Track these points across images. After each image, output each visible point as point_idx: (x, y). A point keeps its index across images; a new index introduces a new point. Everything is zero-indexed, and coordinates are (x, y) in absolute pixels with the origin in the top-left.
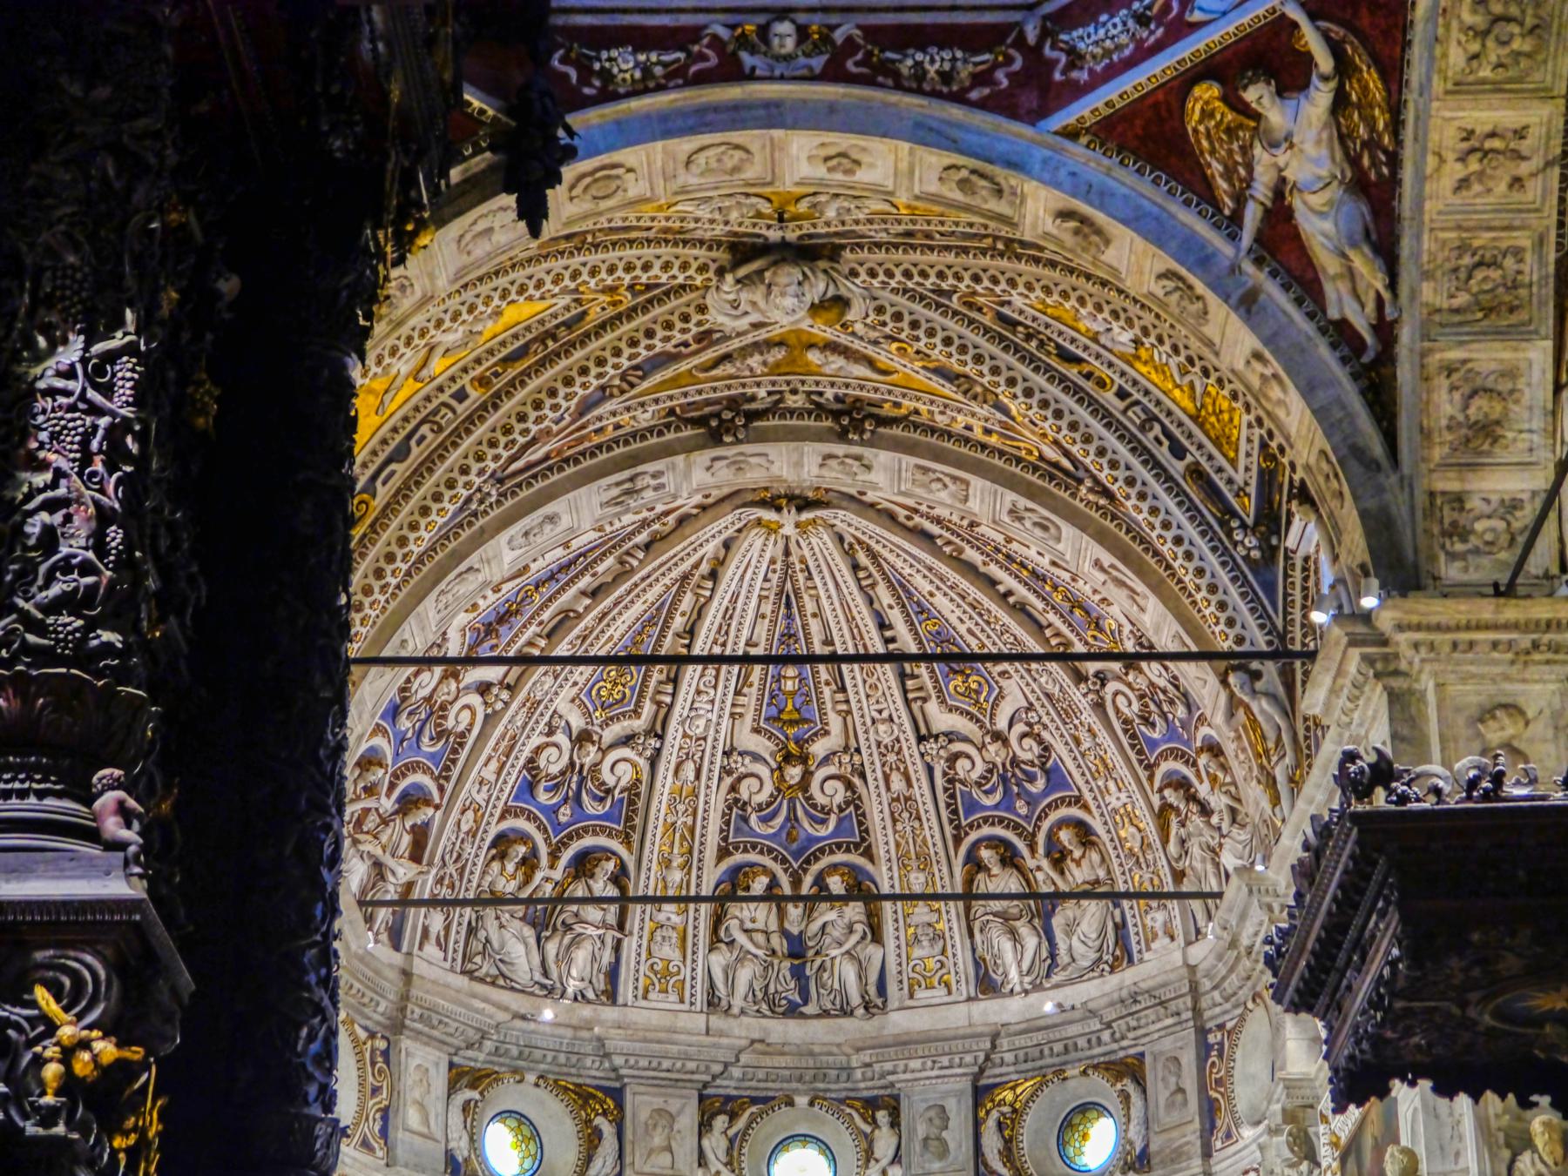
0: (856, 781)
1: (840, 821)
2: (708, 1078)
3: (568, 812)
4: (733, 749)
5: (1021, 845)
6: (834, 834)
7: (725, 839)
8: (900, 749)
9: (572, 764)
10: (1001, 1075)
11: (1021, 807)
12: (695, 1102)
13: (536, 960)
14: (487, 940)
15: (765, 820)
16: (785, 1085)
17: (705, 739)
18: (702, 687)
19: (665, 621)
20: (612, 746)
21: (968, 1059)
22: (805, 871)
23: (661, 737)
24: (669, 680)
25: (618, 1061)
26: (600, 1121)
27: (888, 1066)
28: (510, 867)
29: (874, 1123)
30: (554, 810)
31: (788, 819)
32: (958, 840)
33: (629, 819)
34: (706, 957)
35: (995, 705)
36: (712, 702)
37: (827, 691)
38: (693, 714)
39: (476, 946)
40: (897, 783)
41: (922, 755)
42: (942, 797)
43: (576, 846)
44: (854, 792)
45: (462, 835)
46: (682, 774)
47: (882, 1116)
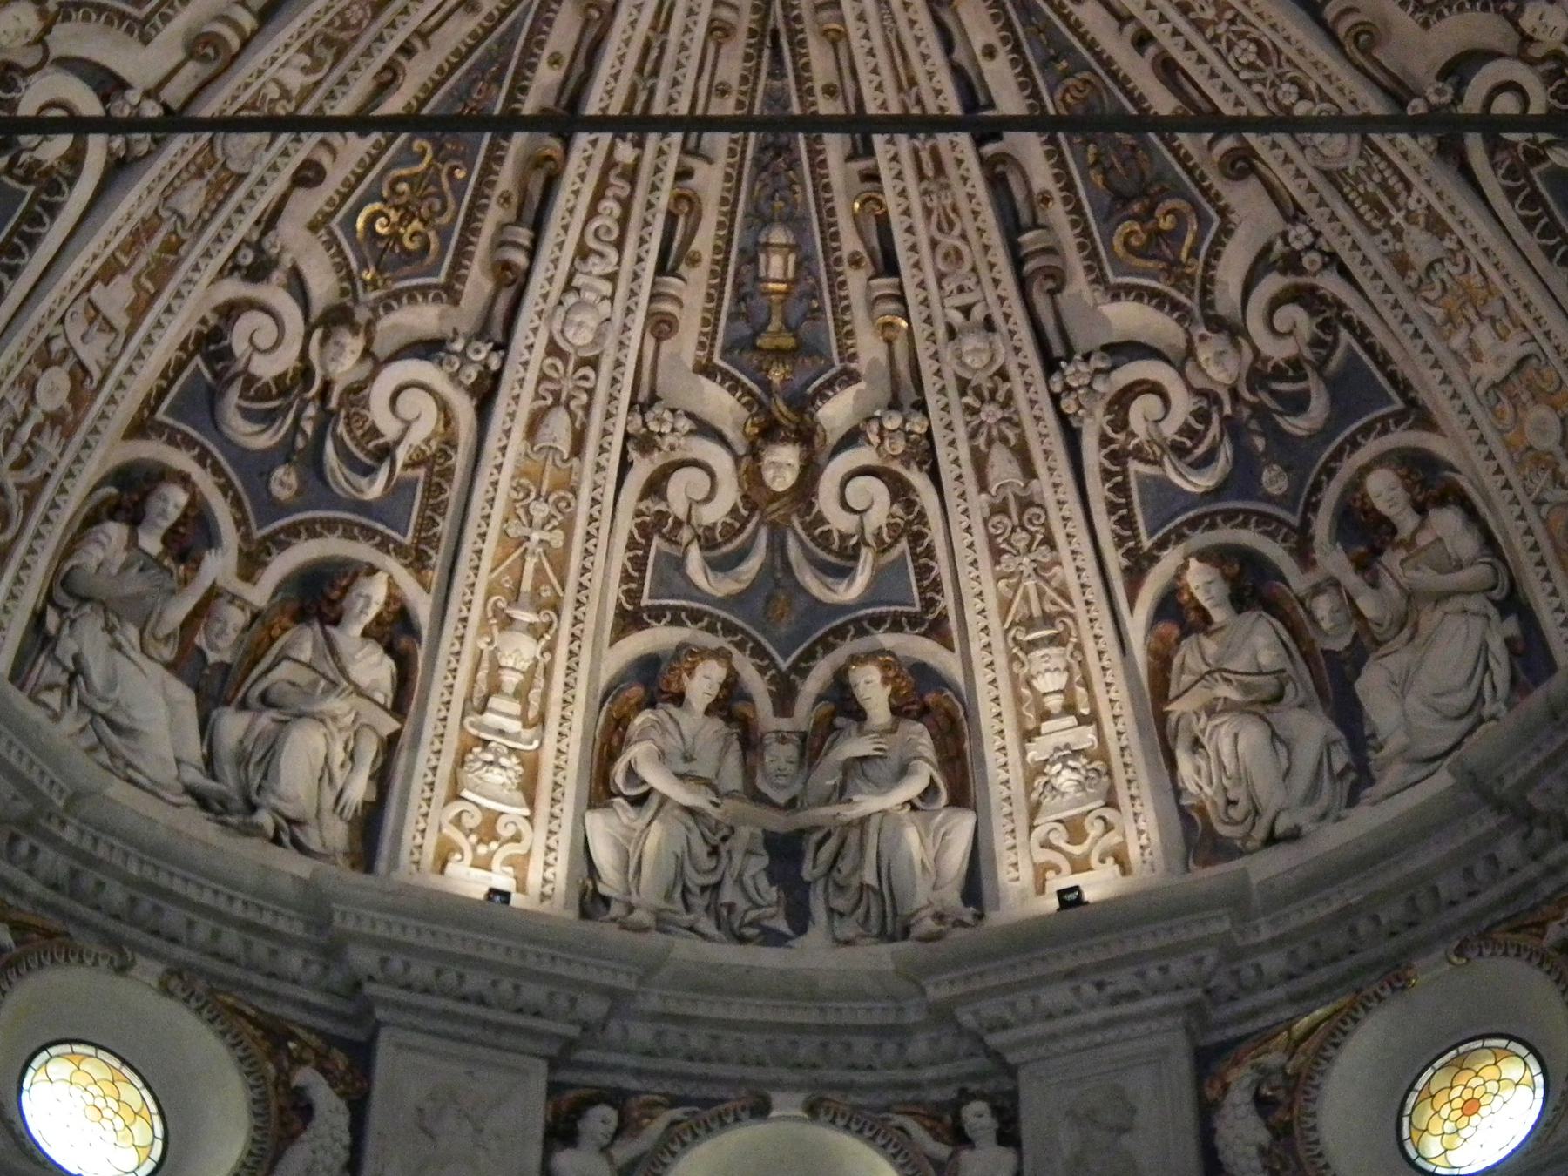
0: (917, 479)
1: (878, 574)
2: (574, 1031)
3: (292, 480)
4: (654, 399)
5: (1275, 551)
6: (863, 603)
7: (633, 595)
8: (1010, 396)
9: (305, 372)
10: (1254, 1014)
11: (1274, 480)
12: (537, 1083)
13: (194, 749)
14: (77, 672)
15: (721, 565)
16: (752, 1072)
17: (594, 363)
18: (592, 243)
19: (518, 75)
20: (395, 356)
21: (1179, 968)
22: (804, 673)
23: (502, 347)
24: (519, 221)
25: (363, 959)
26: (306, 1076)
27: (991, 1009)
28: (151, 543)
29: (960, 1138)
30: (257, 467)
31: (766, 570)
32: (1135, 575)
33: (427, 523)
34: (579, 820)
35: (1215, 254)
36: (612, 278)
37: (856, 282)
38: (571, 299)
39: (46, 671)
40: (1002, 467)
41: (1055, 399)
42: (1098, 491)
43: (304, 552)
44: (909, 505)
45: (36, 416)
46: (544, 439)
47: (977, 1116)
